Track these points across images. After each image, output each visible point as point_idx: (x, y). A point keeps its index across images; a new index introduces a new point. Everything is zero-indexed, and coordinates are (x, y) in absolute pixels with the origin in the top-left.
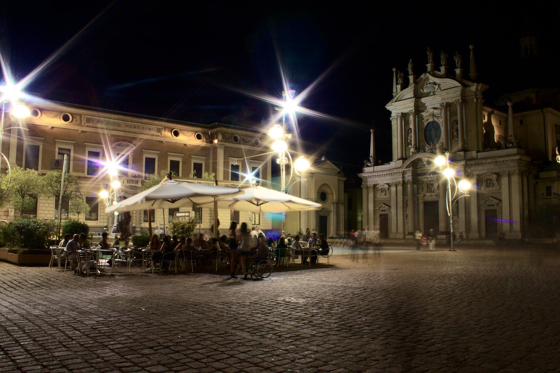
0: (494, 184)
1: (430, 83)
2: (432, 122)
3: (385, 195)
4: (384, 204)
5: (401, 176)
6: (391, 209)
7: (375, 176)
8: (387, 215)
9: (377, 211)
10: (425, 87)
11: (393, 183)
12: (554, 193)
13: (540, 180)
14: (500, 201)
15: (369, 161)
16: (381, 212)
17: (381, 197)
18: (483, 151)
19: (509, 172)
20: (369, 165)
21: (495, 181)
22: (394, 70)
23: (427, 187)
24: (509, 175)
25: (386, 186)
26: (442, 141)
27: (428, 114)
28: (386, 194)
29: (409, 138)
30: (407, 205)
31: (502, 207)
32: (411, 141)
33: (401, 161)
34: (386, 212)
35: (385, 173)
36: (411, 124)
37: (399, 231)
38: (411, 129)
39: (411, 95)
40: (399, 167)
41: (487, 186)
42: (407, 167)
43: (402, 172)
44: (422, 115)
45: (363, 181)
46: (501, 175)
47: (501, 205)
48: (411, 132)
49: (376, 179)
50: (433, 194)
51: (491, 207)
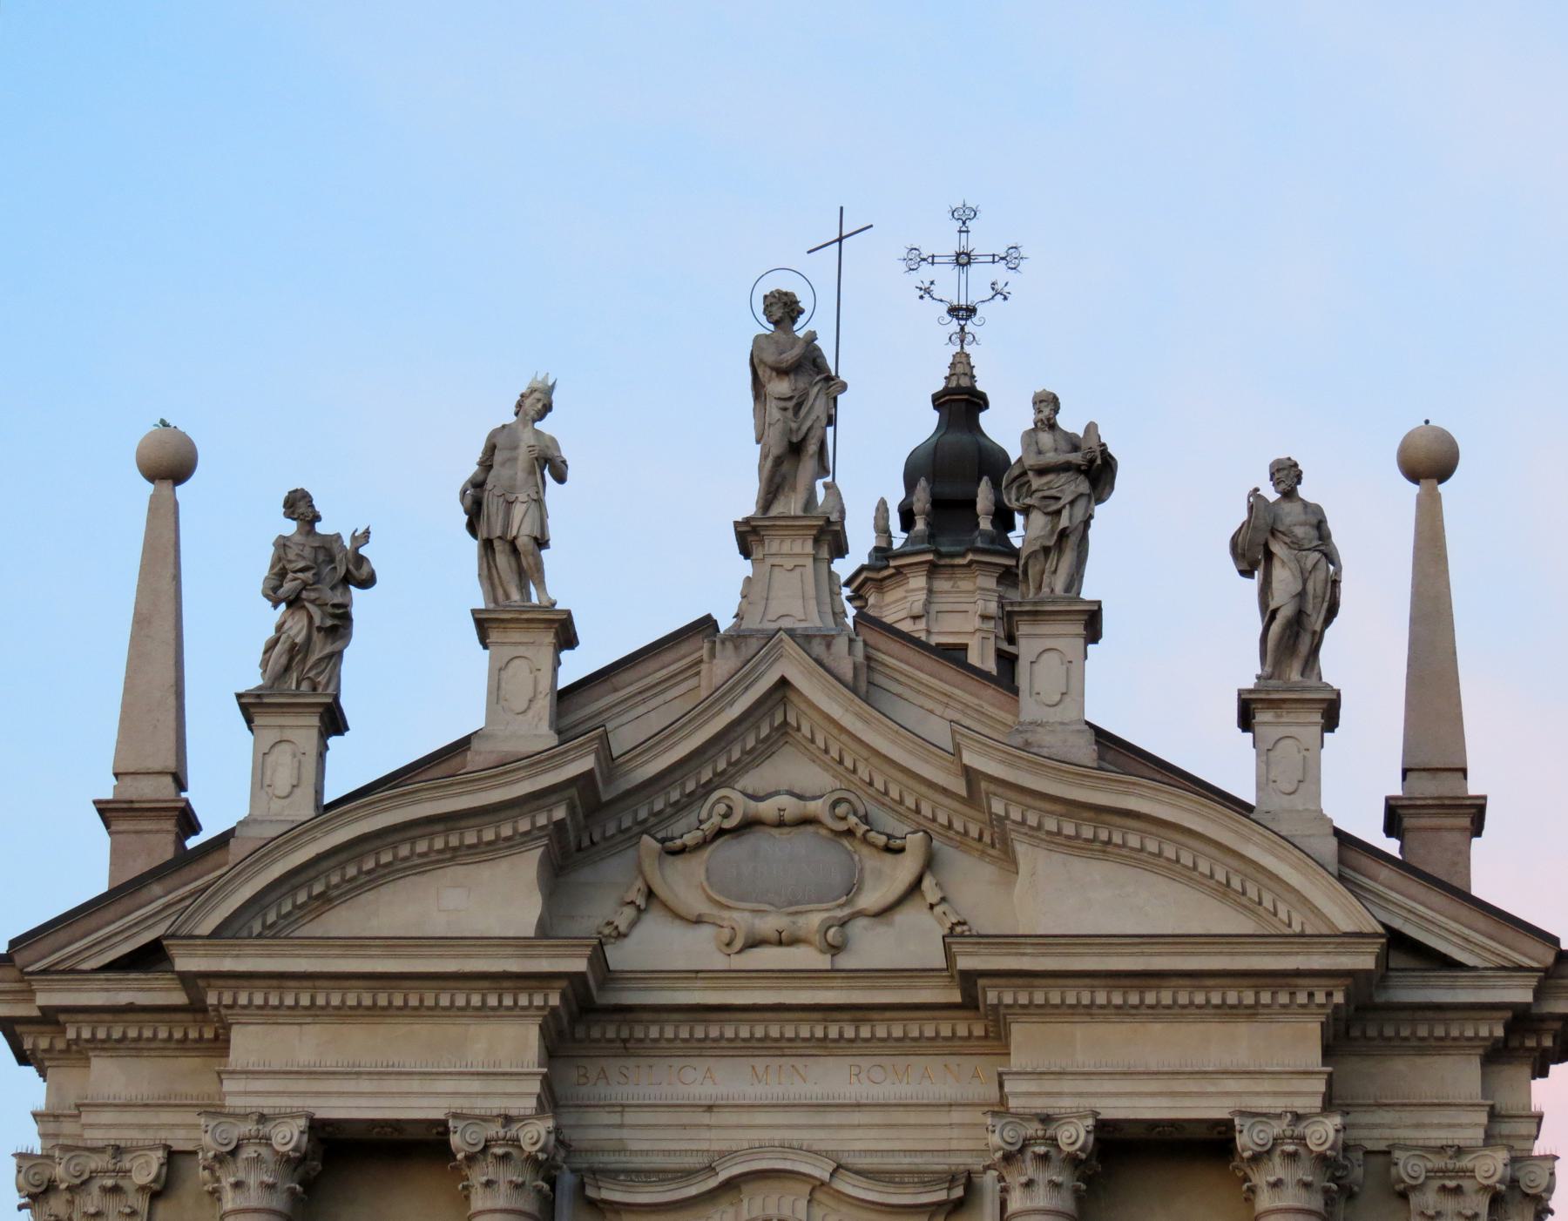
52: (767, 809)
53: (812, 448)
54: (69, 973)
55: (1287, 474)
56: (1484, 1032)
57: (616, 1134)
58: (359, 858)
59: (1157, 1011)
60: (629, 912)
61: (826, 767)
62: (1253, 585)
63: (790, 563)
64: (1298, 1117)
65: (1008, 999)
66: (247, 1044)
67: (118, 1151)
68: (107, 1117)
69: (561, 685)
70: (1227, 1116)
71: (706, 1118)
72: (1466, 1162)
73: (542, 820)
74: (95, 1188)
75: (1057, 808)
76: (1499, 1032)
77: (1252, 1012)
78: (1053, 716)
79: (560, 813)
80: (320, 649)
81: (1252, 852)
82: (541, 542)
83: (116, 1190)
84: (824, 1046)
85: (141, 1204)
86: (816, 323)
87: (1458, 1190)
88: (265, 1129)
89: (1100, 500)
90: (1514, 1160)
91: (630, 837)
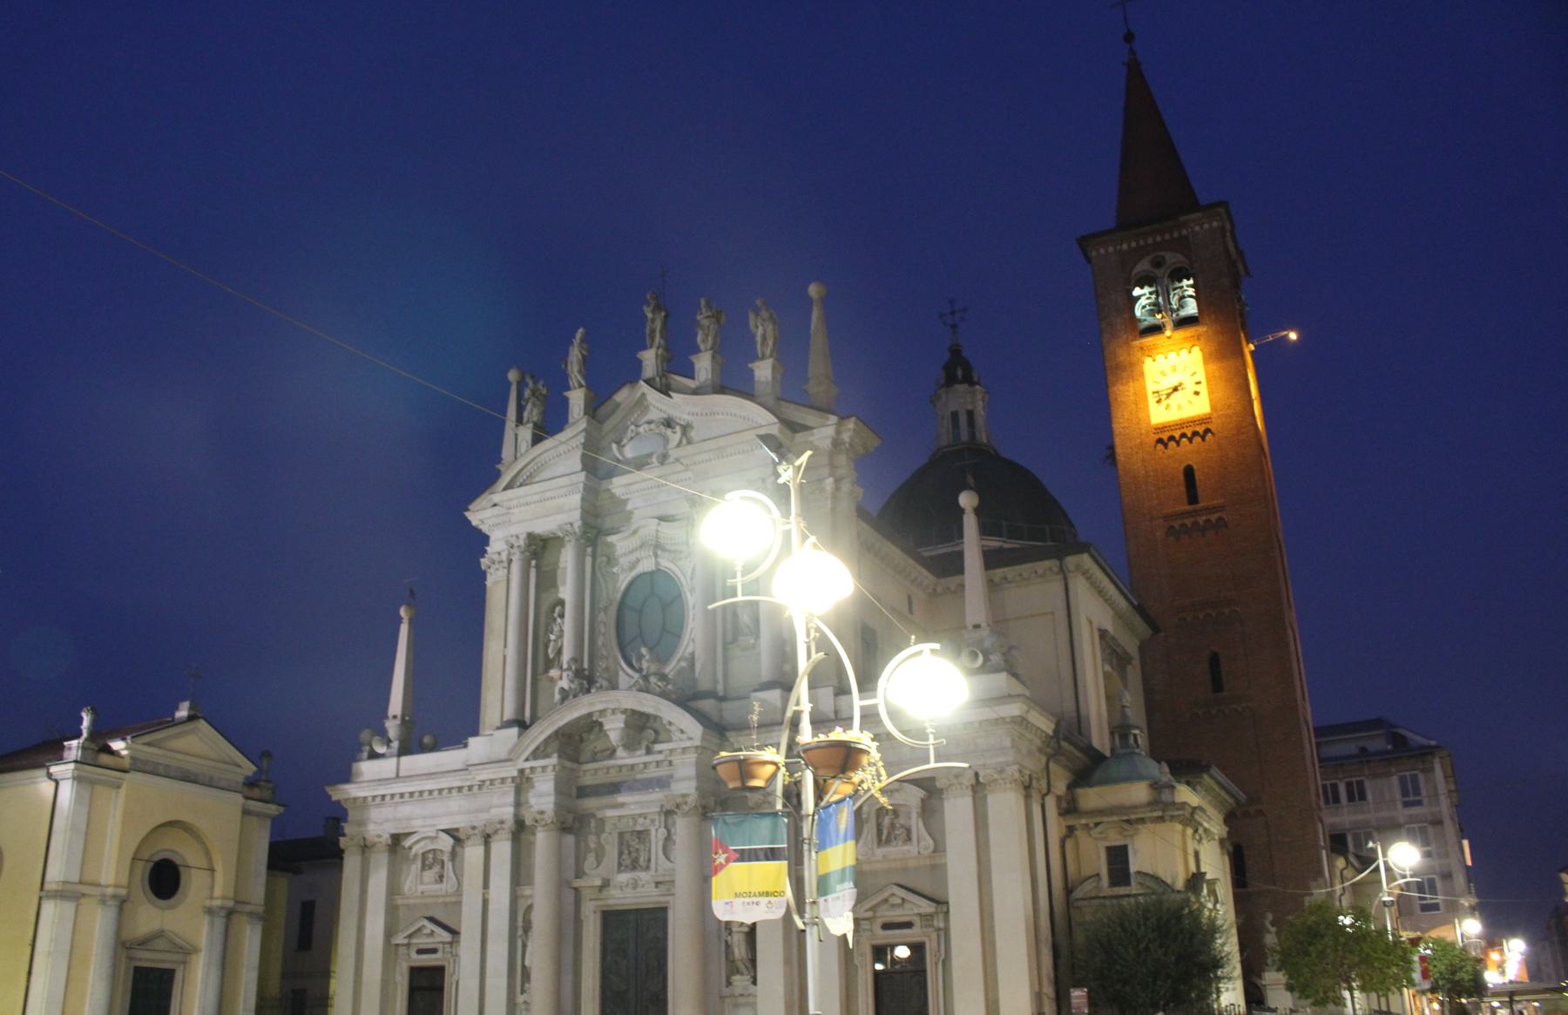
0: (909, 831)
1: (650, 422)
2: (651, 574)
3: (436, 882)
4: (432, 920)
5: (511, 798)
6: (458, 942)
7: (402, 795)
8: (439, 971)
9: (402, 950)
10: (630, 434)
11: (474, 828)
12: (1139, 873)
14: (941, 903)
15: (382, 733)
16: (414, 956)
17: (421, 888)
19: (977, 774)
20: (381, 749)
21: (914, 815)
22: (513, 376)
23: (621, 844)
26: (690, 649)
27: (634, 541)
28: (441, 877)
29: (552, 637)
30: (527, 928)
31: (947, 930)
32: (559, 652)
33: (514, 731)
34: (439, 955)
35: (444, 783)
36: (564, 583)
38: (561, 603)
39: (575, 462)
42: (536, 755)
43: (513, 779)
44: (611, 545)
45: (350, 818)
46: (941, 791)
47: (942, 925)
48: (562, 616)
49: (406, 810)
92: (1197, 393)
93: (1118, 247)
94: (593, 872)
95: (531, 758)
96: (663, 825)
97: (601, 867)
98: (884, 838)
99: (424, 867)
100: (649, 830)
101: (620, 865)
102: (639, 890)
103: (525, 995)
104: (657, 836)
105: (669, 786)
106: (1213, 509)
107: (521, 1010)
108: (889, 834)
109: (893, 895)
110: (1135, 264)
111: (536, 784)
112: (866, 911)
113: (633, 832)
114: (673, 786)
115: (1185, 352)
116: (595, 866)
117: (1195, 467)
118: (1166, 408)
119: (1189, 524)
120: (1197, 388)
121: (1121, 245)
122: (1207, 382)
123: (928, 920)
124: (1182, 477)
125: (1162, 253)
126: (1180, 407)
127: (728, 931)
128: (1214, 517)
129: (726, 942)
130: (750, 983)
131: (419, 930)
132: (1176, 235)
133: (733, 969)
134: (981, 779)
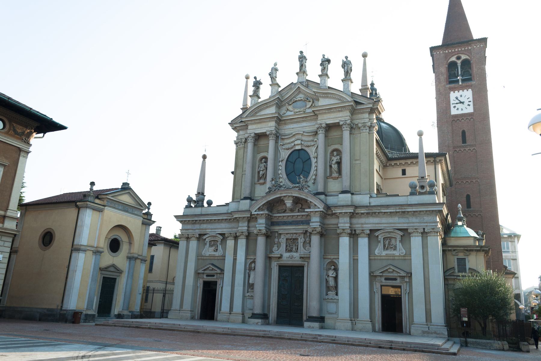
0: (395, 247)
4: (213, 264)
8: (215, 283)
11: (231, 234)
12: (470, 269)
13: (450, 249)
16: (205, 277)
18: (377, 197)
24: (424, 234)
25: (221, 237)
28: (217, 250)
34: (215, 277)
37: (235, 310)
38: (266, 158)
40: (244, 209)
41: (385, 248)
42: (259, 209)
49: (204, 226)
50: (295, 254)
51: (390, 281)
52: (297, 99)
53: (304, 65)
54: (236, 123)
55: (346, 57)
56: (368, 111)
57: (284, 132)
58: (259, 108)
59: (332, 112)
60: (286, 111)
61: (303, 94)
62: (343, 69)
63: (301, 76)
64: (346, 121)
65: (317, 113)
66: (249, 127)
67: (241, 139)
68: (241, 136)
69: (279, 91)
70: (338, 121)
71: (292, 129)
72: (366, 124)
73: (275, 103)
74: (240, 143)
75: (322, 94)
76: (369, 110)
77: (341, 111)
78: (323, 85)
79: (276, 102)
80: (257, 91)
81: (341, 95)
82: (276, 77)
83: (241, 142)
84: (303, 121)
85: (244, 143)
86: (305, 54)
87: (365, 127)
88: (251, 134)
89: (329, 64)
90: (371, 123)
91: (285, 105)
92: (469, 105)
93: (444, 52)
94: (277, 252)
95: (257, 211)
96: (303, 237)
97: (279, 250)
98: (386, 248)
99: (211, 246)
100: (298, 239)
101: (286, 250)
102: (293, 259)
103: (249, 293)
104: (301, 240)
105: (309, 224)
106: (471, 146)
107: (247, 298)
108: (388, 247)
109: (390, 268)
110: (450, 58)
111: (258, 220)
112: (381, 273)
113: (291, 239)
114: (311, 224)
115: (465, 90)
116: (277, 249)
117: (466, 131)
118: (457, 110)
119: (462, 150)
120: (469, 103)
121: (445, 51)
122: (473, 101)
123: (403, 278)
124: (461, 134)
125: (459, 55)
126: (462, 110)
127: (327, 276)
128: (472, 149)
129: (326, 280)
130: (335, 295)
131: (208, 268)
132: (466, 48)
133: (328, 288)
134: (426, 231)
